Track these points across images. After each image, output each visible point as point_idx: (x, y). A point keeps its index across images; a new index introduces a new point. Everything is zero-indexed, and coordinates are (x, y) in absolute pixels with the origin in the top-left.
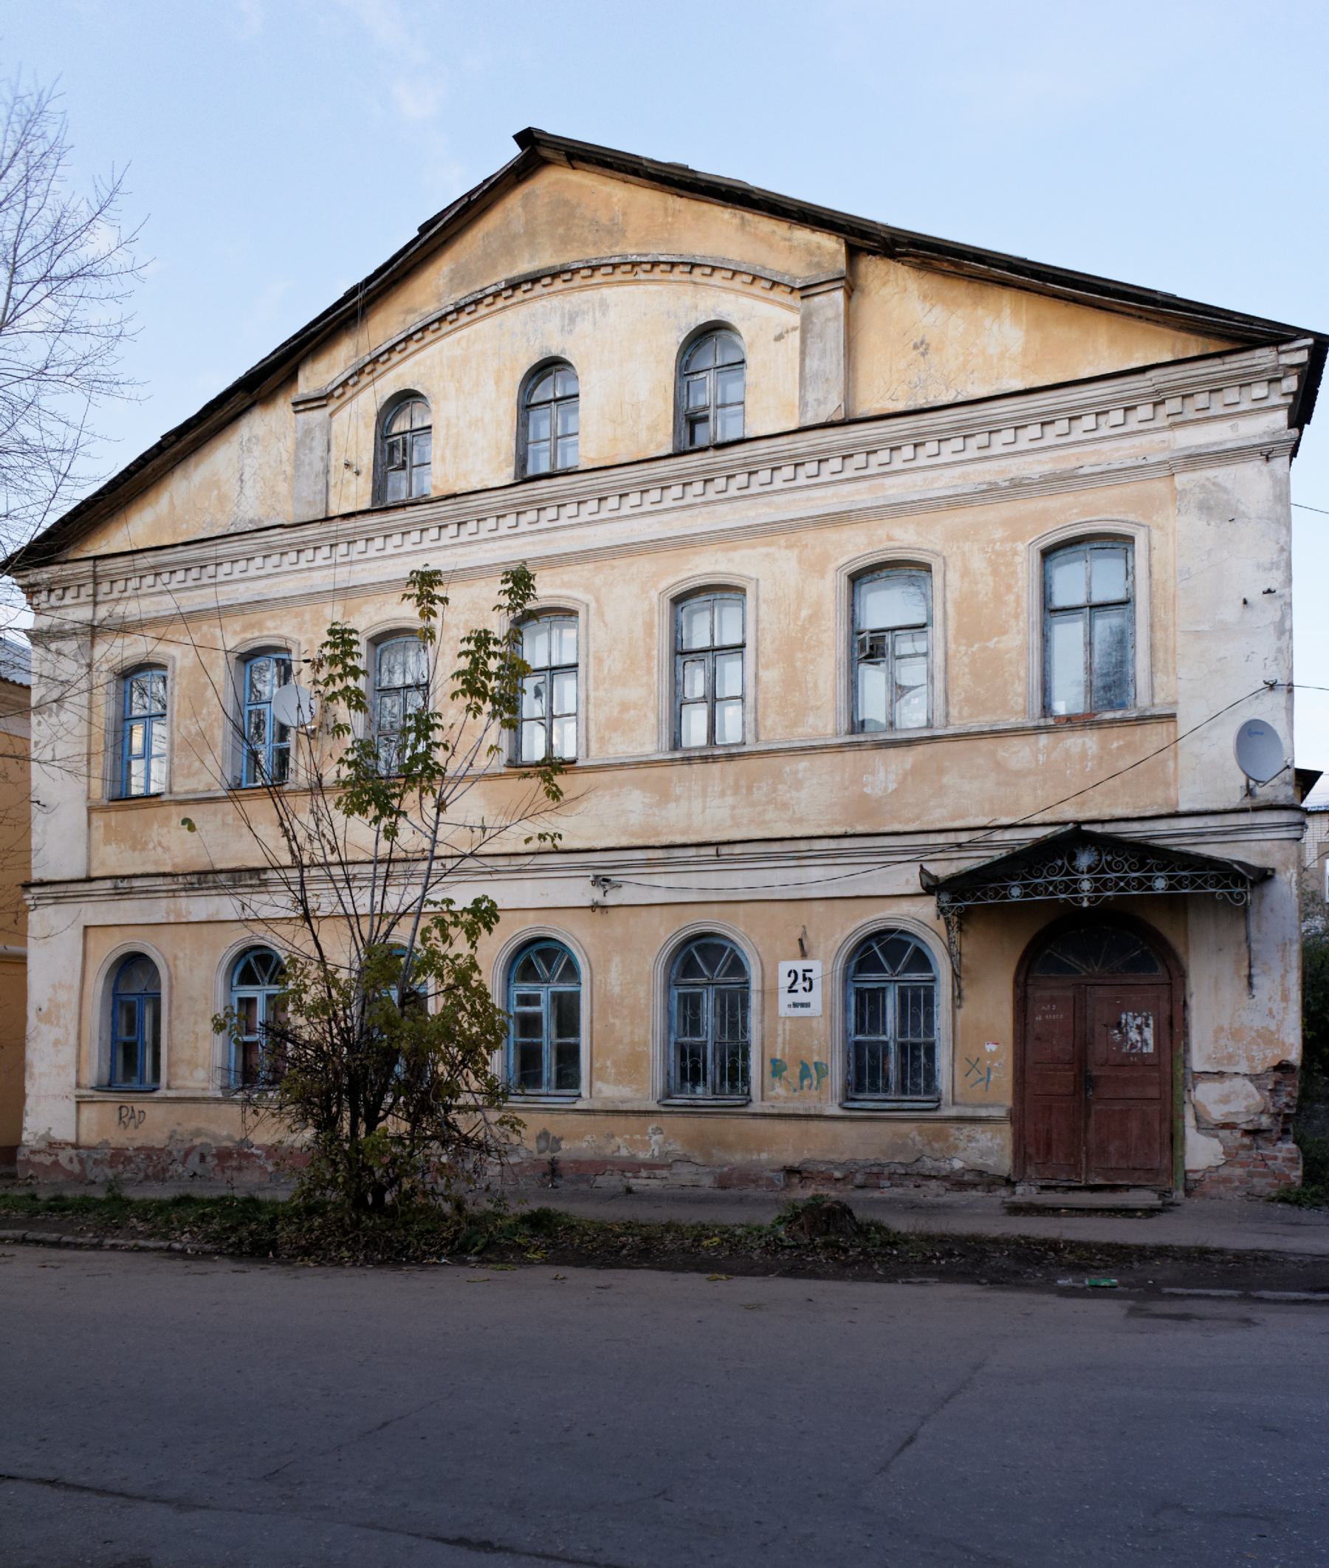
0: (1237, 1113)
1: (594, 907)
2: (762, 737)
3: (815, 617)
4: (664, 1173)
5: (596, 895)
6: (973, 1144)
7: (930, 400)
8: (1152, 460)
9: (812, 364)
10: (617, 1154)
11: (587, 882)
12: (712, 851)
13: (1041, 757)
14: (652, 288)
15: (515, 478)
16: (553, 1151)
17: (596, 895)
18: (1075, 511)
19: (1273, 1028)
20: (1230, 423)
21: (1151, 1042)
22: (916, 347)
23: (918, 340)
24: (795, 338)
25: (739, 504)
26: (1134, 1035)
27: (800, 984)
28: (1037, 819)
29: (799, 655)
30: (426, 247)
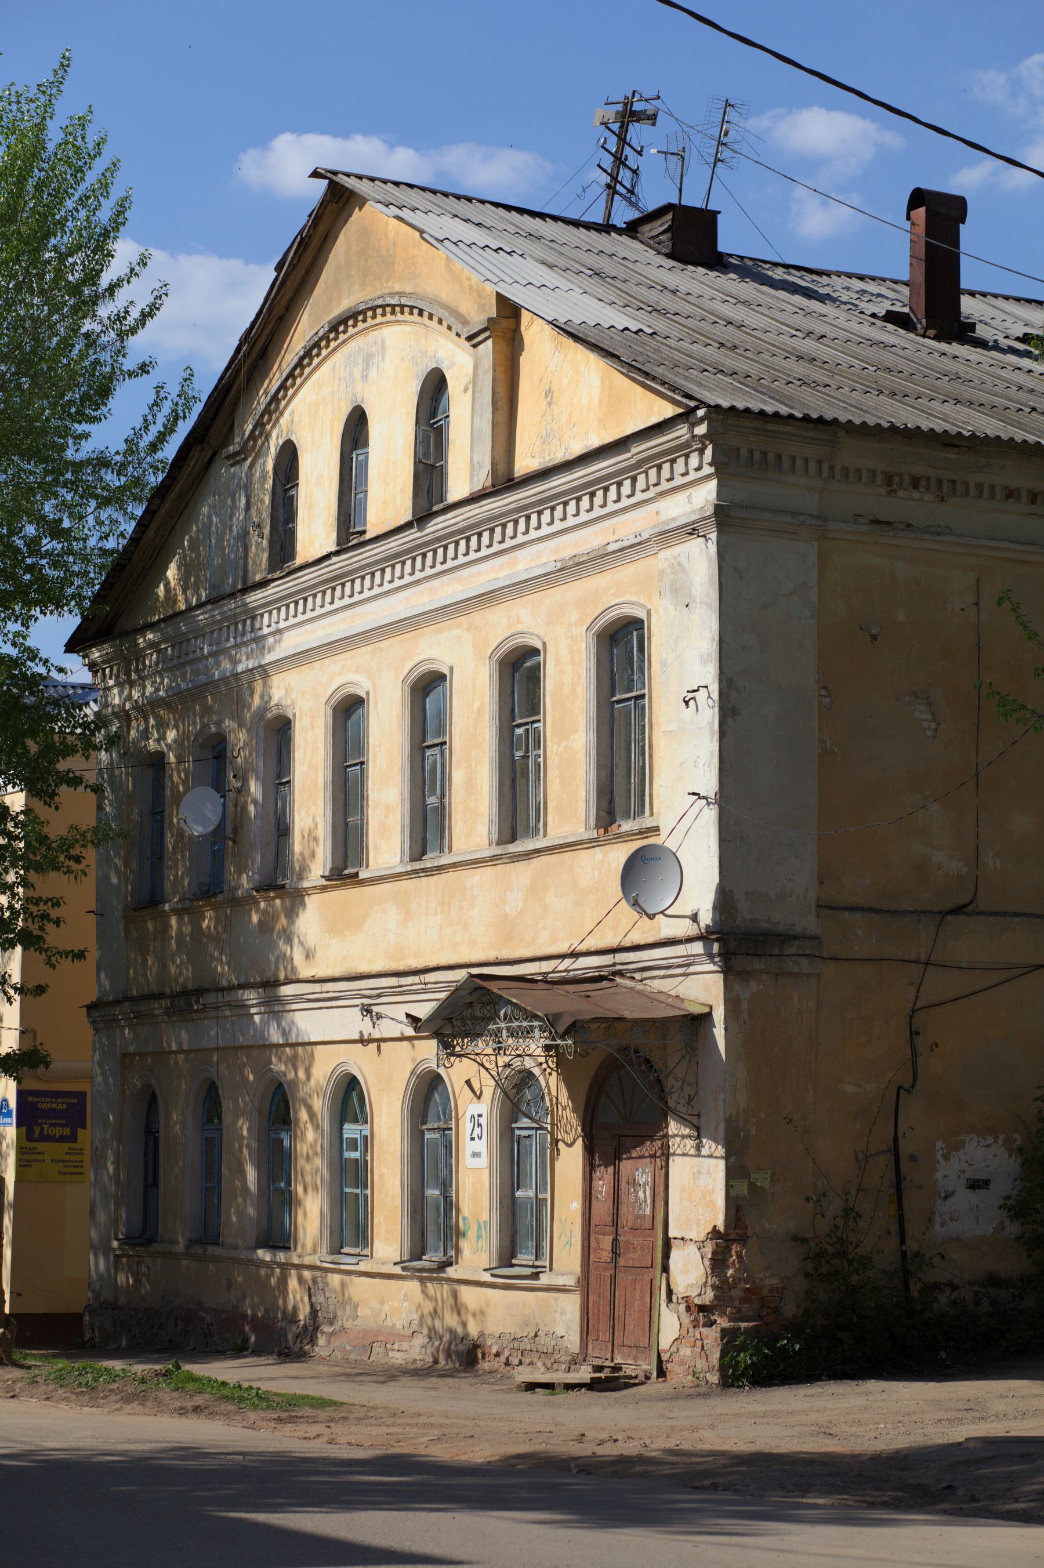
0: (691, 1286)
1: (363, 1041)
2: (454, 848)
3: (480, 708)
4: (405, 1345)
5: (366, 1027)
6: (563, 1317)
7: (552, 456)
8: (645, 536)
9: (477, 421)
10: (385, 1324)
11: (357, 1009)
12: (416, 979)
13: (596, 875)
14: (407, 328)
15: (338, 545)
16: (354, 1320)
17: (366, 1027)
18: (612, 591)
19: (710, 1187)
20: (687, 493)
21: (649, 1202)
22: (546, 396)
23: (547, 387)
24: (470, 386)
25: (445, 579)
26: (641, 1194)
27: (477, 1131)
28: (592, 943)
29: (473, 753)
30: (288, 283)
